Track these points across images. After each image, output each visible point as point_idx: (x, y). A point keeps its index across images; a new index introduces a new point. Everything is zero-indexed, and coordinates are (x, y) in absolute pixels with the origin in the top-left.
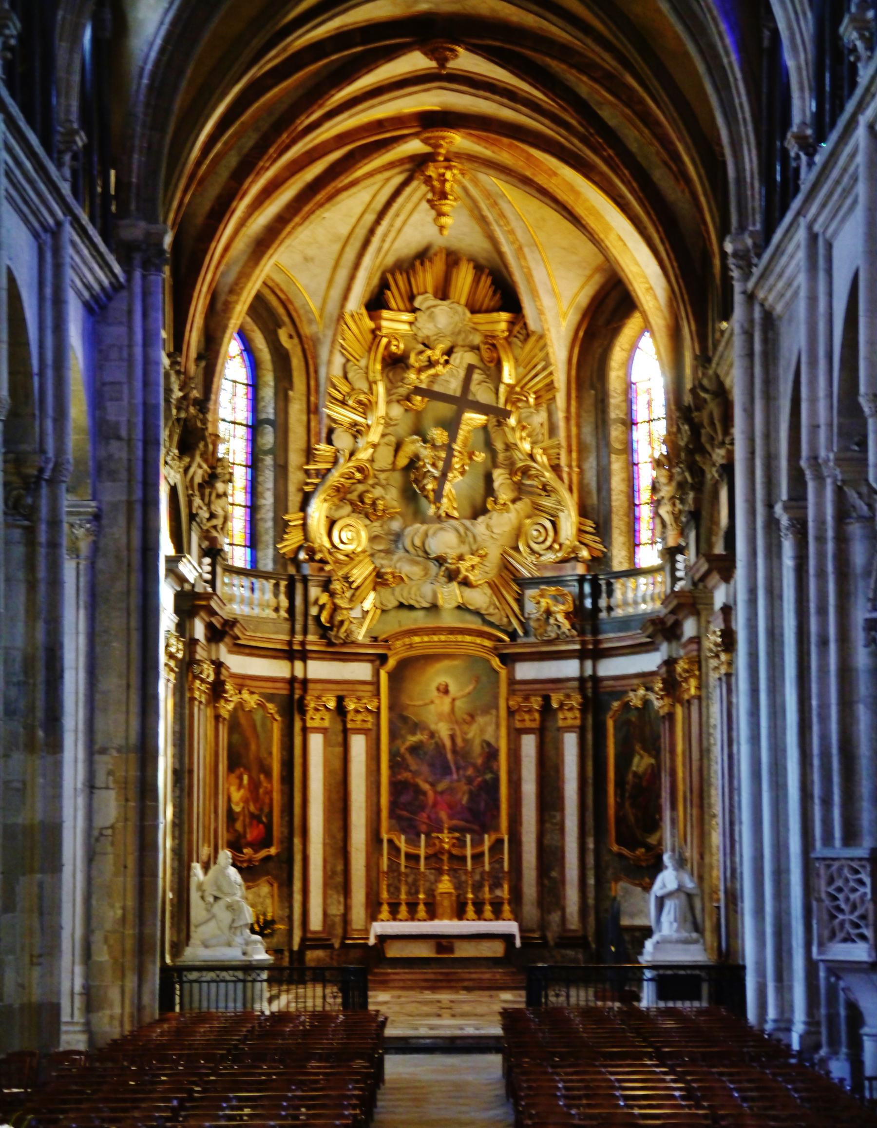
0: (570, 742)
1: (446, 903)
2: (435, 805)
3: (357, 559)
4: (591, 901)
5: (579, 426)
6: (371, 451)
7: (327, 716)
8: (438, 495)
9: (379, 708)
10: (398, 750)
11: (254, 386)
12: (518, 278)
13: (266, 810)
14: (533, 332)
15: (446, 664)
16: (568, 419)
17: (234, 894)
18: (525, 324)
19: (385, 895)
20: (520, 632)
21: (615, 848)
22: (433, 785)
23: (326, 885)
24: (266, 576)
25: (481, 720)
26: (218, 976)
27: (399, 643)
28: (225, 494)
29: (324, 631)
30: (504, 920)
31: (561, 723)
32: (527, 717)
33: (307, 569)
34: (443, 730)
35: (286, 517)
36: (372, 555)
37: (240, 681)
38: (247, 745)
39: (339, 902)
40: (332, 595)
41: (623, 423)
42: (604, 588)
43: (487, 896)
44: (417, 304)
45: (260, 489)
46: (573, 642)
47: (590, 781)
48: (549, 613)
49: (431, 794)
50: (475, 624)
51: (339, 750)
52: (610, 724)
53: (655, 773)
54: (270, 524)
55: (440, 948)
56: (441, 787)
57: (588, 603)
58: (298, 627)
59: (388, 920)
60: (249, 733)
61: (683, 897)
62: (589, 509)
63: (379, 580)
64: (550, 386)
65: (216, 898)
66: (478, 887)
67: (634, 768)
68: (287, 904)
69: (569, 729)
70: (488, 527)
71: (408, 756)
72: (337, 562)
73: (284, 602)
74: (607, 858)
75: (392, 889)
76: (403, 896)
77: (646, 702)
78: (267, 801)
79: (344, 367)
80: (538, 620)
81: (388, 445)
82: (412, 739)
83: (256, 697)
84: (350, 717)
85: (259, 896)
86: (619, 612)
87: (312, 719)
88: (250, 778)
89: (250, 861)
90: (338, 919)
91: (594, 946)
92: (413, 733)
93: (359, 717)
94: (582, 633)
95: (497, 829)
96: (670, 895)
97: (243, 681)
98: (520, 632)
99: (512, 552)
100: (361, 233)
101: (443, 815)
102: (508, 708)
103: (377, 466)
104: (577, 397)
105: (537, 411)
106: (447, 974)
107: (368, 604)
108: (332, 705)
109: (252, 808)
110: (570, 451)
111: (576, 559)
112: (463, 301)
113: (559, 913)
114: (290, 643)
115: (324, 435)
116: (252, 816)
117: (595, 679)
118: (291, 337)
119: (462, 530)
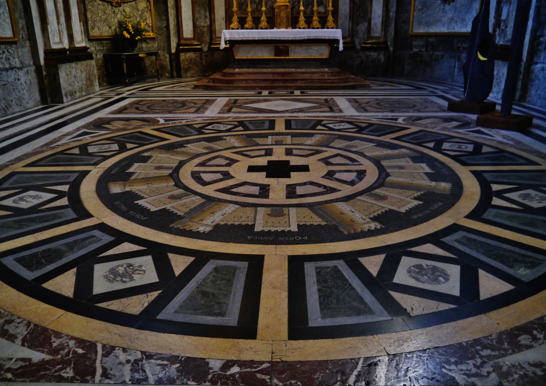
1: (283, 14)
4: (392, 14)
30: (328, 28)
39: (206, 17)
59: (238, 29)
68: (164, 17)
85: (138, 10)
90: (205, 29)
91: (391, 49)
106: (283, 74)
113: (366, 24)
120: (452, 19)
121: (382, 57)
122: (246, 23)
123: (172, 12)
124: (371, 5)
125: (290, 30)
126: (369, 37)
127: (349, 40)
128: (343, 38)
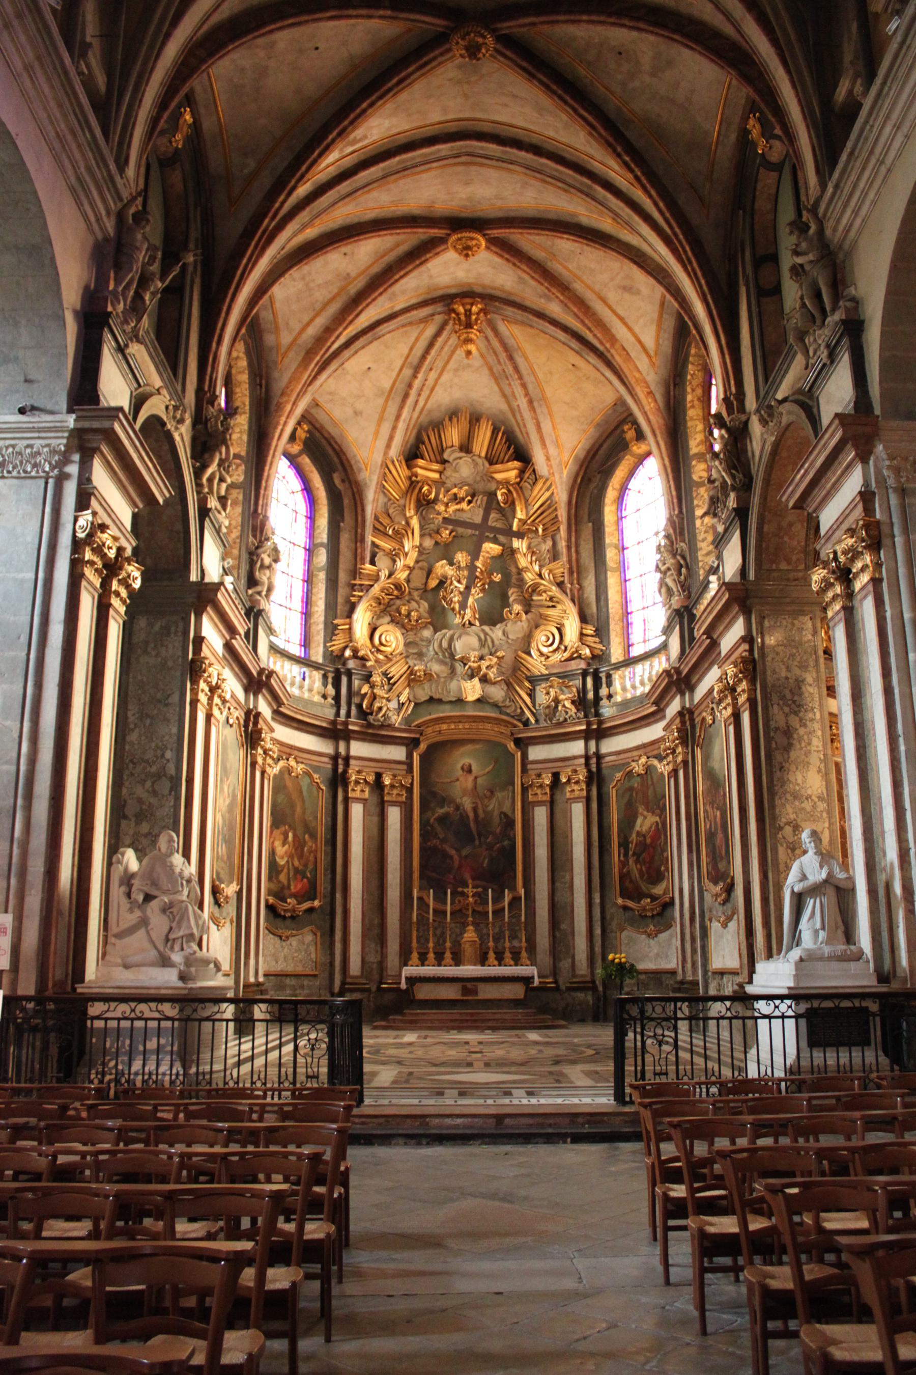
0: (578, 810)
2: (460, 866)
3: (395, 660)
5: (577, 552)
6: (407, 573)
7: (367, 790)
8: (463, 606)
9: (412, 784)
10: (428, 820)
11: (311, 518)
12: (531, 427)
13: (310, 866)
14: (541, 477)
15: (469, 747)
16: (569, 548)
17: (177, 892)
18: (534, 470)
19: (414, 944)
20: (532, 720)
21: (620, 901)
22: (457, 850)
23: (364, 935)
24: (315, 666)
25: (499, 795)
26: (133, 1010)
27: (430, 730)
28: (269, 567)
29: (363, 714)
31: (568, 795)
32: (539, 791)
33: (351, 664)
34: (467, 803)
35: (336, 622)
36: (407, 657)
37: (288, 750)
38: (292, 806)
40: (372, 687)
41: (616, 547)
42: (604, 680)
43: (507, 944)
44: (446, 456)
45: (314, 598)
46: (580, 724)
47: (596, 843)
48: (557, 701)
49: (456, 857)
50: (493, 714)
51: (375, 819)
52: (613, 794)
53: (661, 831)
54: (321, 626)
55: (465, 991)
56: (465, 852)
57: (591, 695)
58: (343, 712)
60: (295, 796)
61: (831, 892)
62: (589, 618)
63: (412, 679)
64: (555, 520)
65: (148, 898)
66: (498, 938)
67: (637, 827)
69: (576, 800)
70: (504, 633)
71: (436, 825)
72: (377, 661)
73: (331, 690)
74: (611, 910)
75: (422, 941)
76: (431, 945)
77: (649, 769)
78: (312, 858)
79: (385, 504)
80: (548, 707)
81: (421, 568)
82: (441, 811)
83: (302, 766)
84: (386, 791)
86: (619, 699)
87: (353, 790)
88: (295, 836)
89: (294, 910)
90: (375, 966)
91: (601, 989)
92: (442, 807)
93: (395, 792)
94: (586, 716)
95: (513, 888)
96: (815, 890)
97: (288, 751)
98: (532, 720)
99: (524, 655)
100: (401, 387)
101: (467, 876)
102: (522, 784)
103: (412, 585)
104: (576, 531)
105: (545, 542)
106: (472, 1015)
107: (403, 699)
108: (371, 778)
109: (296, 863)
110: (571, 572)
111: (580, 657)
112: (483, 454)
113: (570, 960)
114: (334, 723)
115: (368, 559)
116: (297, 870)
117: (599, 756)
118: (343, 481)
119: (483, 637)
120: (657, 955)
121: (590, 998)
122: (426, 959)
123: (338, 946)
124: (573, 939)
125: (479, 967)
126: (574, 976)
127: (550, 980)
128: (539, 977)
